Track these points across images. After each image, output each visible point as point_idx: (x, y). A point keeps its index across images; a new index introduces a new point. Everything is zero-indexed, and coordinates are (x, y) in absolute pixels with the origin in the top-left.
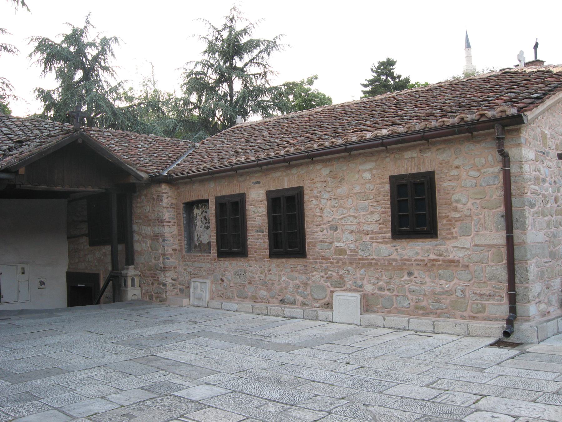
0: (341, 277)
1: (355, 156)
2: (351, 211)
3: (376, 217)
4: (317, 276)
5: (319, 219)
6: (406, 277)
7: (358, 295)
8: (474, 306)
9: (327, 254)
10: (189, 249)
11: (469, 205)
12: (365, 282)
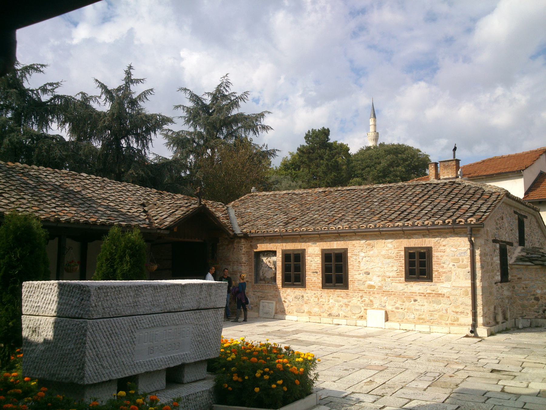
0: (371, 301)
1: (383, 235)
2: (380, 264)
3: (395, 268)
4: (355, 301)
5: (358, 267)
6: (413, 302)
7: (384, 312)
8: (453, 318)
9: (362, 287)
10: (256, 282)
11: (451, 265)
12: (387, 304)
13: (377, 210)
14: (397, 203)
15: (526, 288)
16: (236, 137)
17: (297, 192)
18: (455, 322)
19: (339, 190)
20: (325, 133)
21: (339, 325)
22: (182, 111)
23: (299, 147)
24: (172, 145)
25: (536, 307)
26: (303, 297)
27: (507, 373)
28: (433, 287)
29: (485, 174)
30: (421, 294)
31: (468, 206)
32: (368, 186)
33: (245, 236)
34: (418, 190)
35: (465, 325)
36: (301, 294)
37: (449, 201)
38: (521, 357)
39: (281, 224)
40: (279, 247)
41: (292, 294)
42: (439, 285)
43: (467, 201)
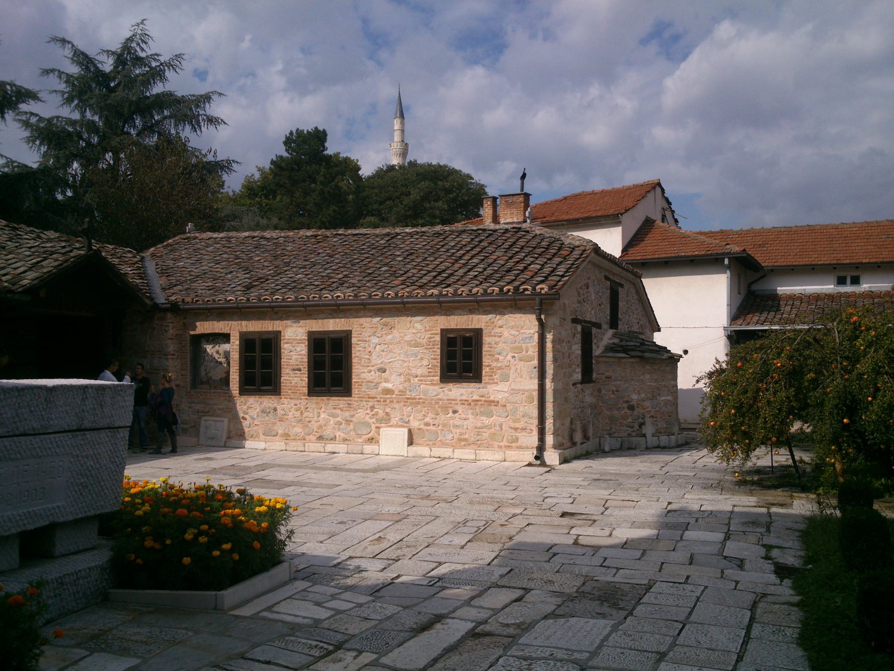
0: (387, 414)
3: (425, 362)
4: (362, 414)
6: (451, 414)
7: (406, 430)
9: (372, 393)
10: (194, 385)
11: (509, 357)
12: (411, 418)
13: (400, 269)
14: (432, 259)
15: (618, 391)
16: (160, 134)
17: (267, 234)
18: (513, 443)
19: (340, 235)
20: (319, 136)
21: (334, 453)
22: (58, 80)
23: (275, 159)
24: (38, 142)
25: (630, 420)
26: (275, 409)
27: (583, 517)
28: (483, 391)
29: (566, 218)
30: (464, 402)
31: (538, 267)
32: (387, 230)
33: (174, 308)
34: (465, 238)
35: (527, 448)
36: (273, 406)
37: (511, 258)
38: (604, 493)
39: (239, 288)
40: (235, 328)
41: (256, 405)
42: (492, 388)
43: (537, 258)
